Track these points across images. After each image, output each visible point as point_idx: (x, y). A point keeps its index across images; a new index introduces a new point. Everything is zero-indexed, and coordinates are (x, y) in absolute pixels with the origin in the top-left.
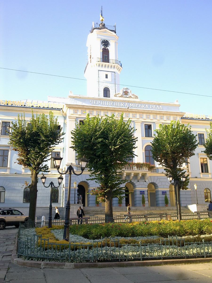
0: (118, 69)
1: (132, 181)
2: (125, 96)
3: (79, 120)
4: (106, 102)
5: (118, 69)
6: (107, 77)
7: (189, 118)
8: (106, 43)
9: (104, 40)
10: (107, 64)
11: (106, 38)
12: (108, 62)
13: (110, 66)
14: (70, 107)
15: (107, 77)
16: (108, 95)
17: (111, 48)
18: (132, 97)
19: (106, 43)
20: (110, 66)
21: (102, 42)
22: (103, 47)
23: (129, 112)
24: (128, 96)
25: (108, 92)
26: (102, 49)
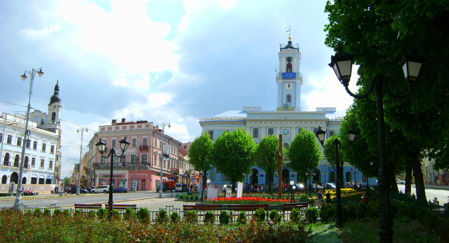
6: (289, 86)
8: (289, 59)
11: (289, 56)
15: (289, 86)
19: (289, 59)
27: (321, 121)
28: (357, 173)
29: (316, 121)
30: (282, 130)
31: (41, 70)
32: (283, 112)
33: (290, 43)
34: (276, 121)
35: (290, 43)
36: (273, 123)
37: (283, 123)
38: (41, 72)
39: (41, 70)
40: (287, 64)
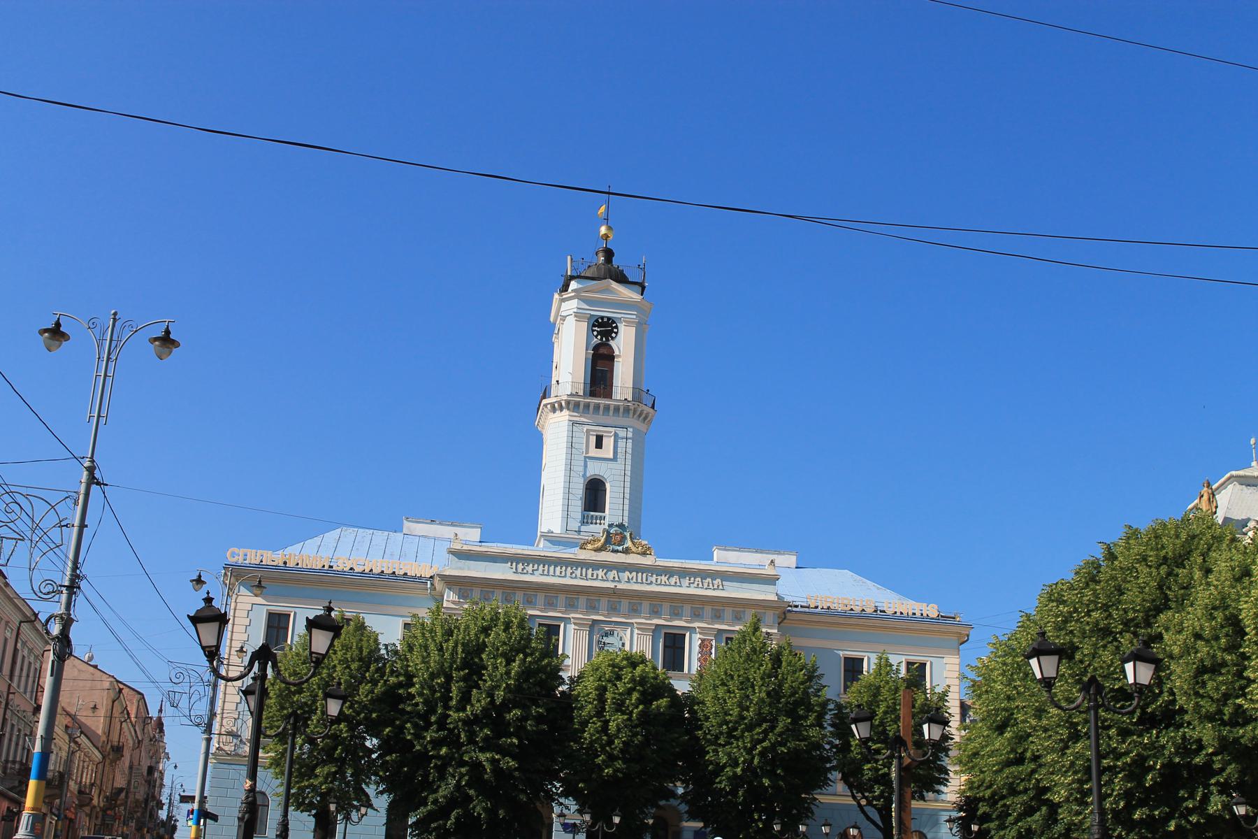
0: (640, 416)
4: (552, 568)
5: (640, 416)
6: (599, 445)
8: (604, 328)
9: (602, 318)
10: (602, 402)
13: (612, 408)
14: (451, 582)
15: (599, 445)
17: (624, 343)
19: (604, 328)
20: (612, 408)
21: (594, 325)
22: (595, 341)
24: (620, 548)
31: (167, 332)
34: (573, 595)
38: (167, 341)
39: (167, 332)
40: (596, 348)
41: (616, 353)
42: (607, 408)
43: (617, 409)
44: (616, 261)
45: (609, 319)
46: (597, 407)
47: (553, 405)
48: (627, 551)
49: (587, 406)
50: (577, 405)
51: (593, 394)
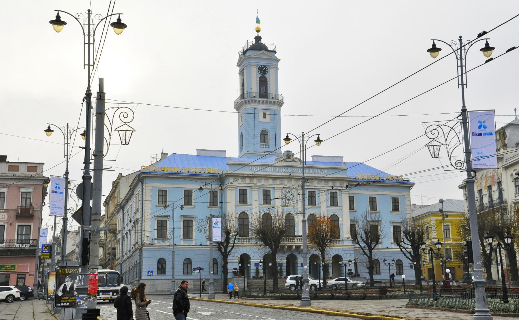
1: (294, 253)
2: (287, 160)
3: (239, 188)
6: (265, 117)
7: (359, 180)
8: (263, 70)
9: (262, 66)
10: (265, 100)
11: (263, 63)
12: (267, 98)
15: (265, 117)
16: (266, 141)
18: (295, 160)
19: (263, 70)
23: (291, 178)
24: (289, 160)
25: (266, 136)
26: (258, 78)
27: (341, 180)
28: (392, 264)
29: (334, 180)
30: (284, 192)
32: (283, 163)
33: (258, 38)
34: (274, 178)
35: (258, 38)
36: (270, 181)
37: (286, 182)
40: (260, 78)
41: (268, 80)
42: (267, 102)
43: (271, 102)
44: (263, 41)
45: (264, 66)
46: (263, 102)
47: (245, 102)
48: (293, 161)
49: (259, 101)
50: (256, 101)
51: (261, 96)
